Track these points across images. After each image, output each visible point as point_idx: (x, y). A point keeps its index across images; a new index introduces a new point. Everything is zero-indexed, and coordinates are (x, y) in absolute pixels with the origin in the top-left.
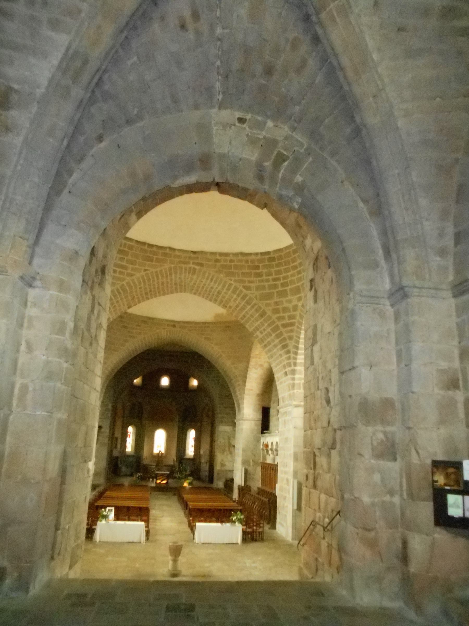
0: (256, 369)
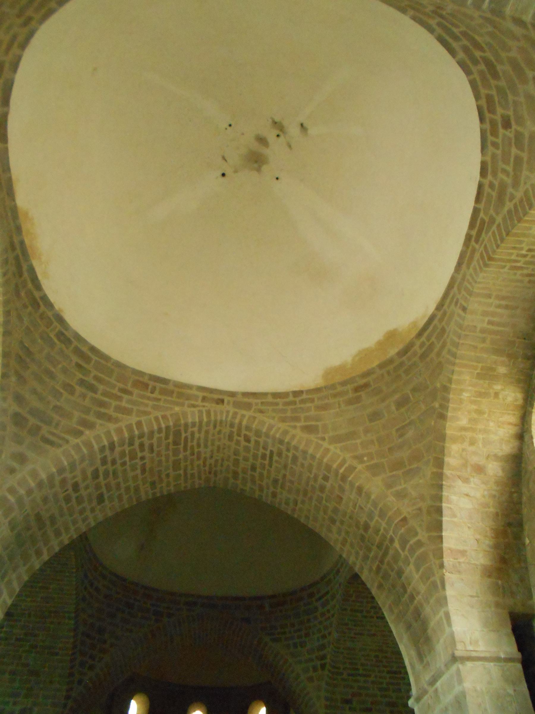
0: (466, 481)
